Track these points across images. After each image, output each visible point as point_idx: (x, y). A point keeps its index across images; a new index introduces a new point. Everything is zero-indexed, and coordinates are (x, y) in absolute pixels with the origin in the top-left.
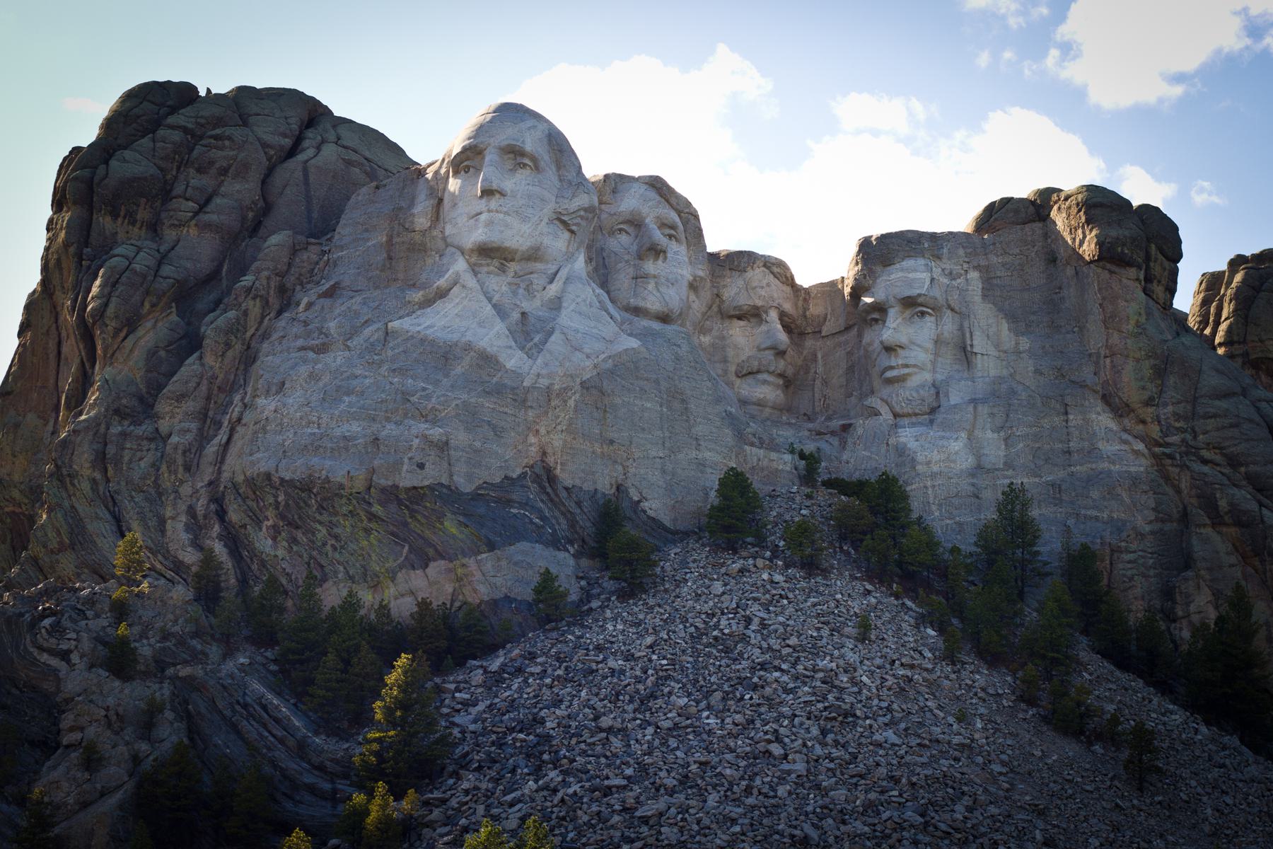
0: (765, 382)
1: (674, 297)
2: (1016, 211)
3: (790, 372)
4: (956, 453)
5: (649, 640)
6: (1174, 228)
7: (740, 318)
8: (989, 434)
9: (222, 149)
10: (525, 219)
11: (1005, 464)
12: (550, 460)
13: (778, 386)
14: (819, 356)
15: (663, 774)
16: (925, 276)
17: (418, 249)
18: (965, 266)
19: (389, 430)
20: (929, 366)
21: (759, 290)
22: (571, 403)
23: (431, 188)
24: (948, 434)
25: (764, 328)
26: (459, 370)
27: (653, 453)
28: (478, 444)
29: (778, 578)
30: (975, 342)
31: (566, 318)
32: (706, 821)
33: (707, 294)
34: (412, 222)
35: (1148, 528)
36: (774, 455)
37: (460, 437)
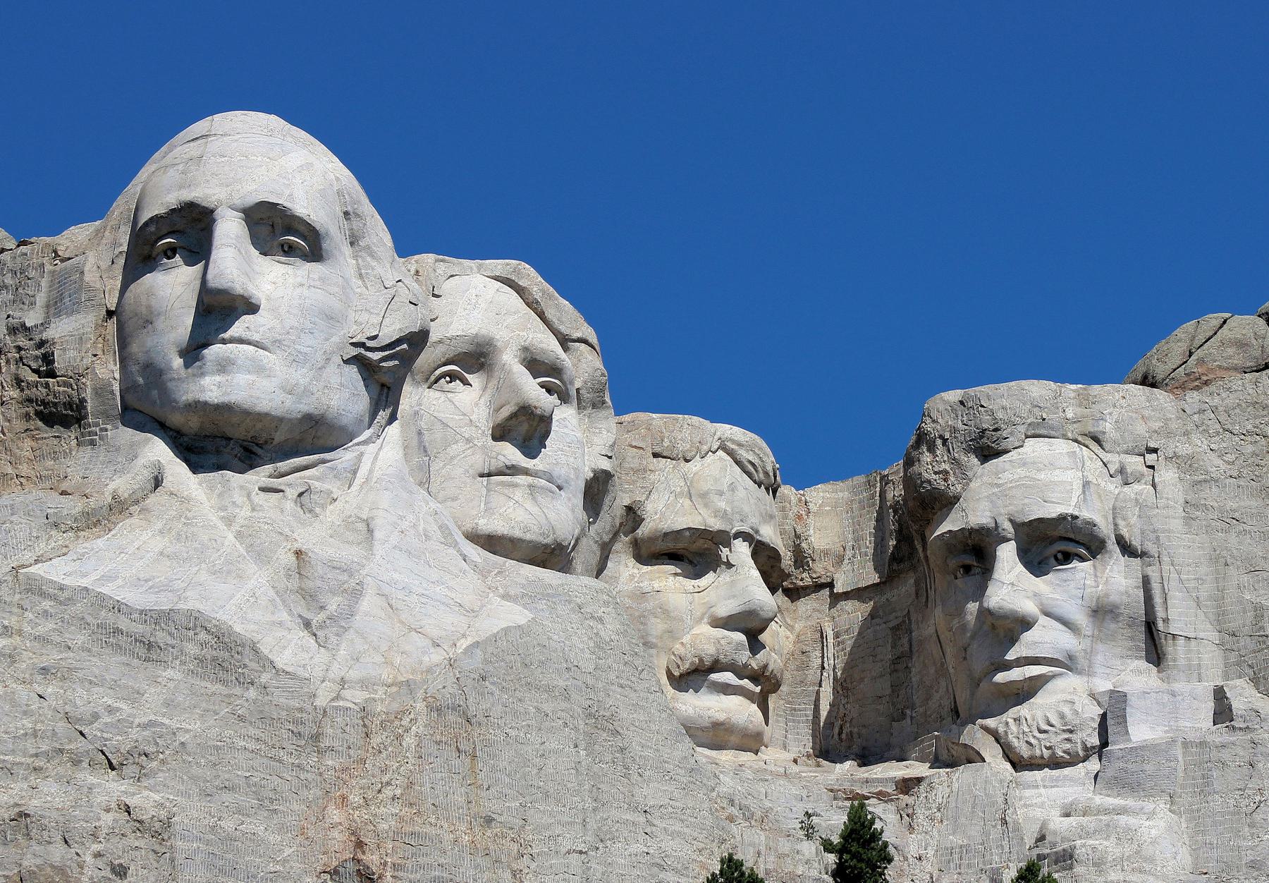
0: (726, 689)
1: (560, 515)
2: (1242, 345)
4: (1154, 842)
7: (672, 557)
8: (1216, 802)
10: (297, 360)
12: (371, 859)
14: (830, 634)
16: (1072, 478)
17: (62, 415)
18: (1151, 458)
19: (48, 797)
21: (715, 498)
22: (409, 741)
24: (1130, 802)
26: (172, 673)
27: (566, 845)
28: (228, 825)
30: (1172, 614)
31: (386, 566)
34: (48, 359)
36: (785, 846)
37: (191, 814)
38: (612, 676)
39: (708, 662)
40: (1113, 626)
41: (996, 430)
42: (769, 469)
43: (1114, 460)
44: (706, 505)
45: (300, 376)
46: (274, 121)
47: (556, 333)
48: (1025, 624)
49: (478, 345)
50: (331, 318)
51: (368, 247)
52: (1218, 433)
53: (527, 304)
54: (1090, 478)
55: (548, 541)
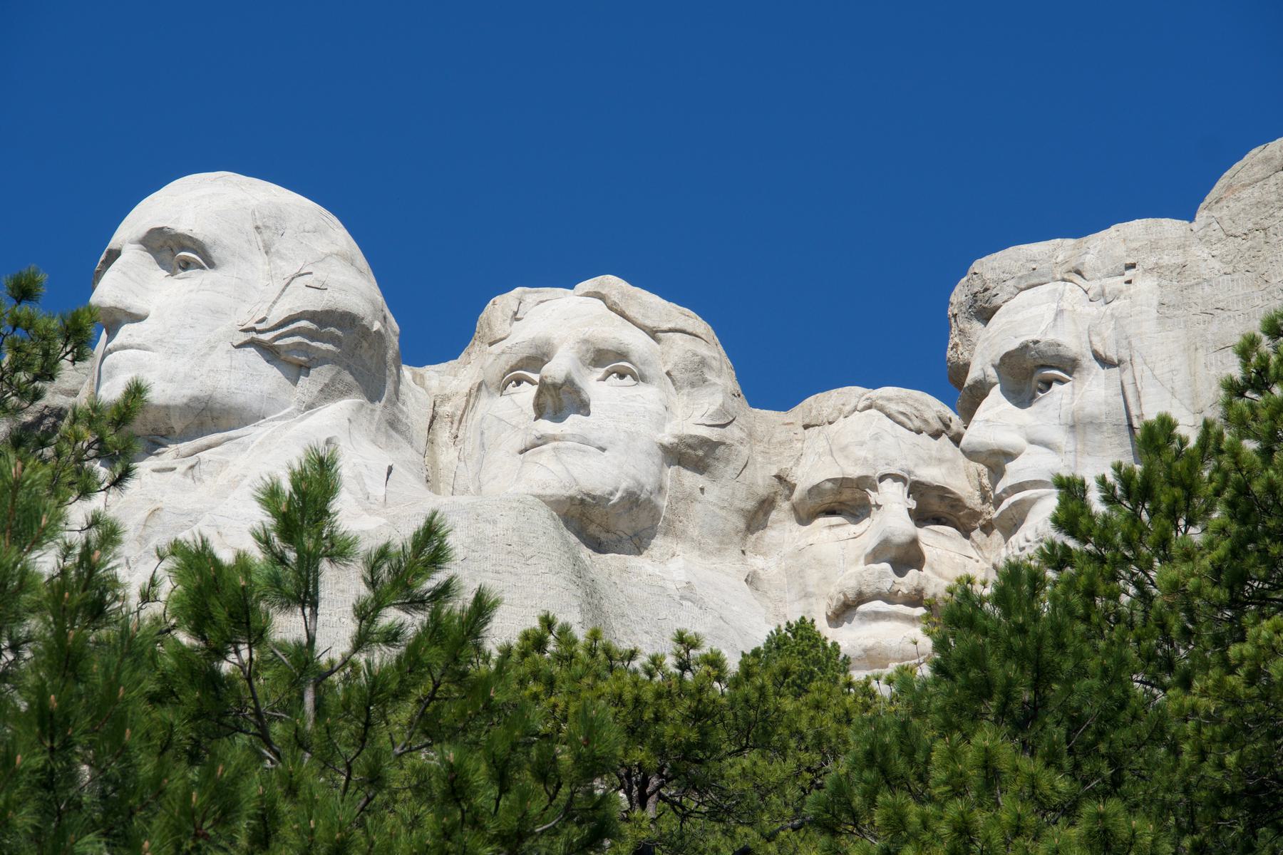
0: (877, 616)
2: (1267, 160)
7: (831, 512)
13: (912, 620)
16: (1048, 311)
18: (1129, 274)
38: (487, 565)
39: (851, 595)
40: (1098, 437)
41: (986, 290)
42: (930, 415)
43: (1094, 286)
44: (846, 457)
45: (180, 365)
47: (643, 328)
48: (1009, 456)
49: (537, 347)
50: (216, 312)
51: (278, 251)
52: (1220, 240)
53: (610, 308)
54: (1065, 305)
55: (572, 492)
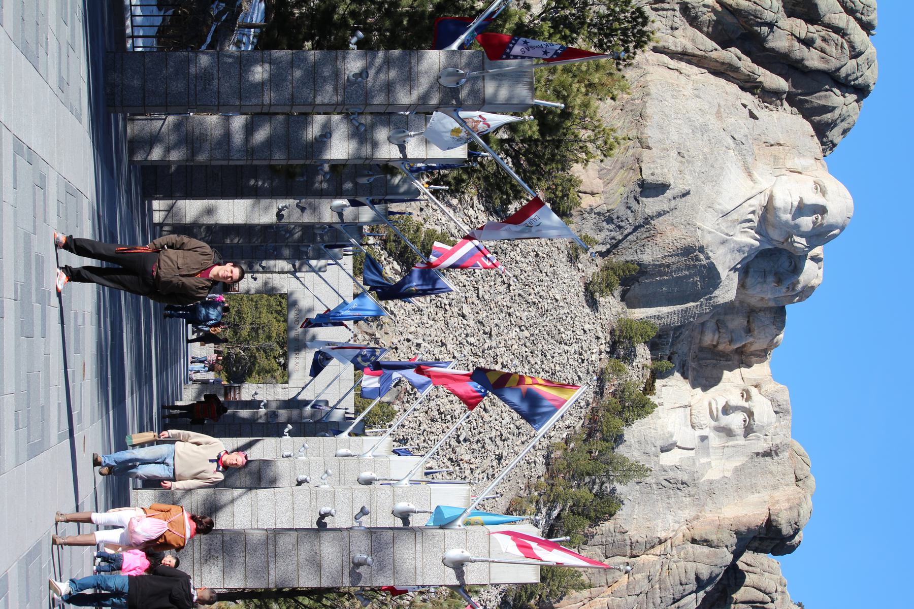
0: (714, 335)
2: (802, 469)
3: (721, 347)
5: (558, 297)
6: (790, 552)
7: (748, 322)
9: (836, 49)
11: (662, 466)
13: (712, 341)
15: (485, 314)
18: (771, 443)
20: (716, 424)
23: (808, 168)
25: (743, 334)
29: (594, 356)
32: (460, 339)
33: (760, 305)
35: (627, 538)
46: (851, 214)
